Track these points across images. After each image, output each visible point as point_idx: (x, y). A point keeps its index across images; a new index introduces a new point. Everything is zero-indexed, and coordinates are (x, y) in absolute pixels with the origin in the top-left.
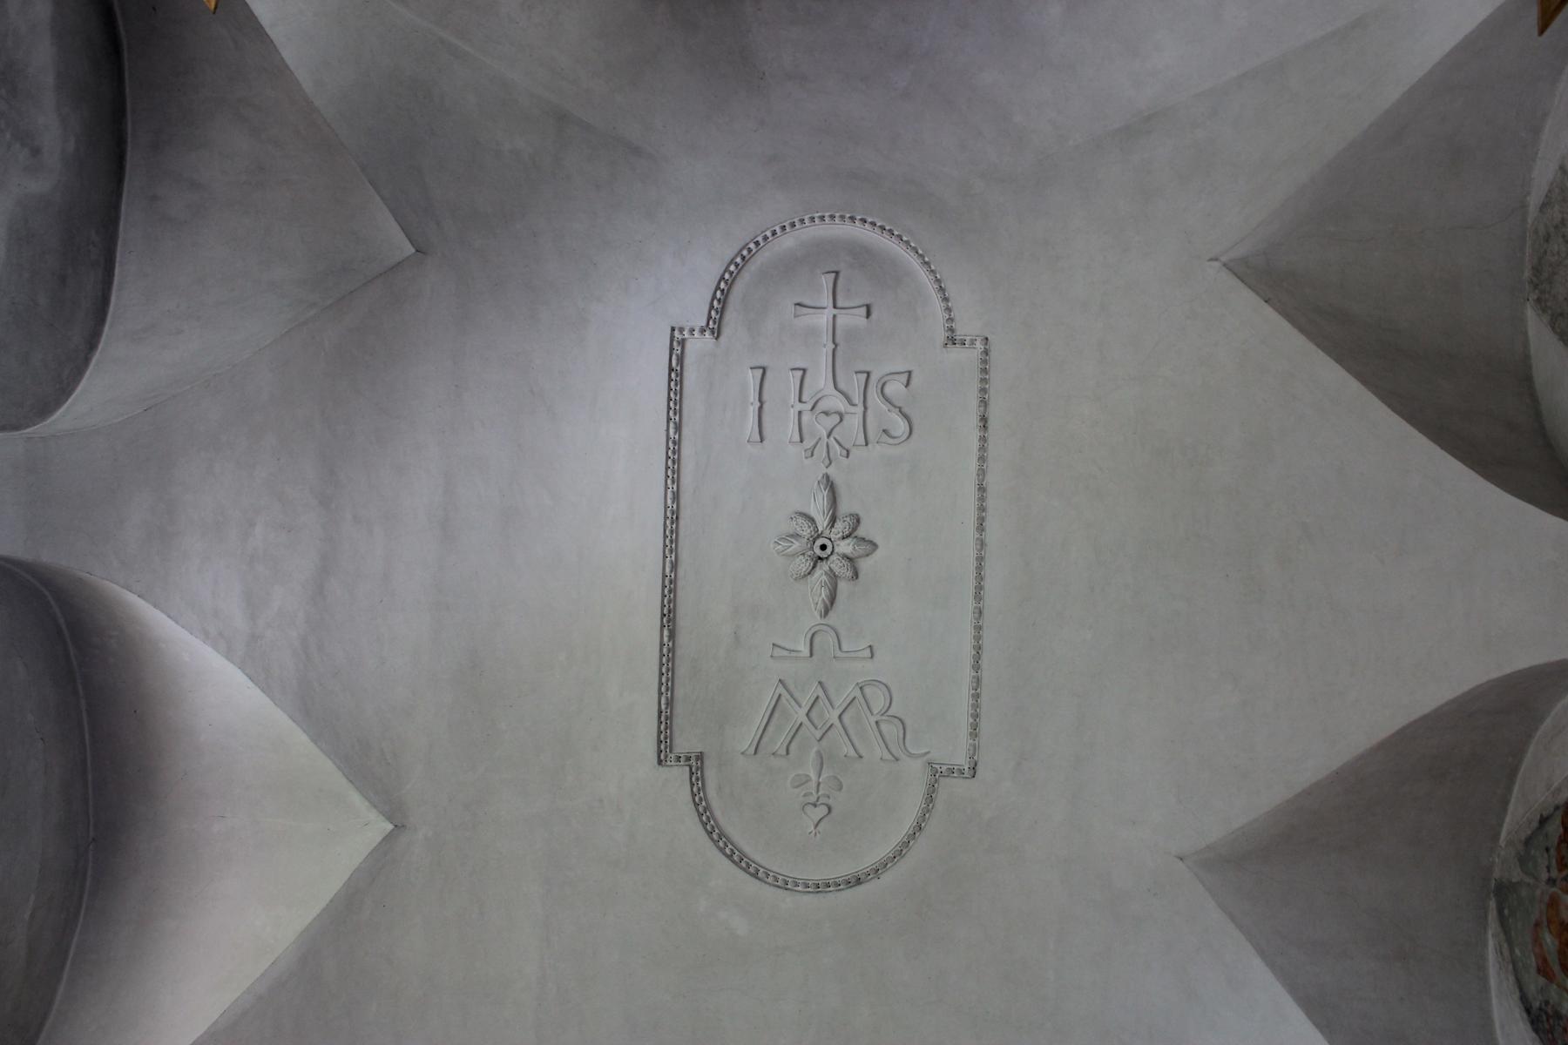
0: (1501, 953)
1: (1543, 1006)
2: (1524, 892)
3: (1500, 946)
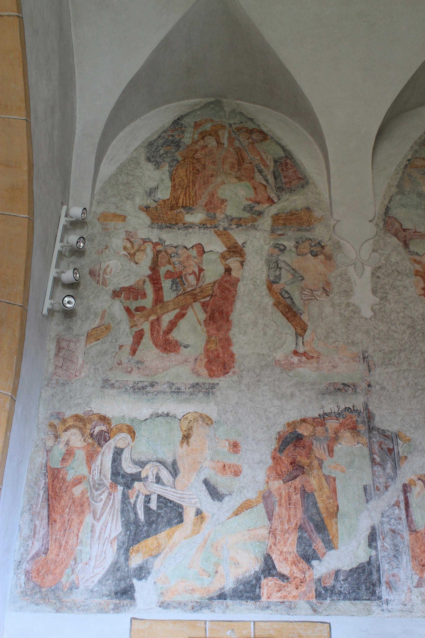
0: (195, 105)
1: (183, 126)
2: (222, 113)
3: (198, 104)
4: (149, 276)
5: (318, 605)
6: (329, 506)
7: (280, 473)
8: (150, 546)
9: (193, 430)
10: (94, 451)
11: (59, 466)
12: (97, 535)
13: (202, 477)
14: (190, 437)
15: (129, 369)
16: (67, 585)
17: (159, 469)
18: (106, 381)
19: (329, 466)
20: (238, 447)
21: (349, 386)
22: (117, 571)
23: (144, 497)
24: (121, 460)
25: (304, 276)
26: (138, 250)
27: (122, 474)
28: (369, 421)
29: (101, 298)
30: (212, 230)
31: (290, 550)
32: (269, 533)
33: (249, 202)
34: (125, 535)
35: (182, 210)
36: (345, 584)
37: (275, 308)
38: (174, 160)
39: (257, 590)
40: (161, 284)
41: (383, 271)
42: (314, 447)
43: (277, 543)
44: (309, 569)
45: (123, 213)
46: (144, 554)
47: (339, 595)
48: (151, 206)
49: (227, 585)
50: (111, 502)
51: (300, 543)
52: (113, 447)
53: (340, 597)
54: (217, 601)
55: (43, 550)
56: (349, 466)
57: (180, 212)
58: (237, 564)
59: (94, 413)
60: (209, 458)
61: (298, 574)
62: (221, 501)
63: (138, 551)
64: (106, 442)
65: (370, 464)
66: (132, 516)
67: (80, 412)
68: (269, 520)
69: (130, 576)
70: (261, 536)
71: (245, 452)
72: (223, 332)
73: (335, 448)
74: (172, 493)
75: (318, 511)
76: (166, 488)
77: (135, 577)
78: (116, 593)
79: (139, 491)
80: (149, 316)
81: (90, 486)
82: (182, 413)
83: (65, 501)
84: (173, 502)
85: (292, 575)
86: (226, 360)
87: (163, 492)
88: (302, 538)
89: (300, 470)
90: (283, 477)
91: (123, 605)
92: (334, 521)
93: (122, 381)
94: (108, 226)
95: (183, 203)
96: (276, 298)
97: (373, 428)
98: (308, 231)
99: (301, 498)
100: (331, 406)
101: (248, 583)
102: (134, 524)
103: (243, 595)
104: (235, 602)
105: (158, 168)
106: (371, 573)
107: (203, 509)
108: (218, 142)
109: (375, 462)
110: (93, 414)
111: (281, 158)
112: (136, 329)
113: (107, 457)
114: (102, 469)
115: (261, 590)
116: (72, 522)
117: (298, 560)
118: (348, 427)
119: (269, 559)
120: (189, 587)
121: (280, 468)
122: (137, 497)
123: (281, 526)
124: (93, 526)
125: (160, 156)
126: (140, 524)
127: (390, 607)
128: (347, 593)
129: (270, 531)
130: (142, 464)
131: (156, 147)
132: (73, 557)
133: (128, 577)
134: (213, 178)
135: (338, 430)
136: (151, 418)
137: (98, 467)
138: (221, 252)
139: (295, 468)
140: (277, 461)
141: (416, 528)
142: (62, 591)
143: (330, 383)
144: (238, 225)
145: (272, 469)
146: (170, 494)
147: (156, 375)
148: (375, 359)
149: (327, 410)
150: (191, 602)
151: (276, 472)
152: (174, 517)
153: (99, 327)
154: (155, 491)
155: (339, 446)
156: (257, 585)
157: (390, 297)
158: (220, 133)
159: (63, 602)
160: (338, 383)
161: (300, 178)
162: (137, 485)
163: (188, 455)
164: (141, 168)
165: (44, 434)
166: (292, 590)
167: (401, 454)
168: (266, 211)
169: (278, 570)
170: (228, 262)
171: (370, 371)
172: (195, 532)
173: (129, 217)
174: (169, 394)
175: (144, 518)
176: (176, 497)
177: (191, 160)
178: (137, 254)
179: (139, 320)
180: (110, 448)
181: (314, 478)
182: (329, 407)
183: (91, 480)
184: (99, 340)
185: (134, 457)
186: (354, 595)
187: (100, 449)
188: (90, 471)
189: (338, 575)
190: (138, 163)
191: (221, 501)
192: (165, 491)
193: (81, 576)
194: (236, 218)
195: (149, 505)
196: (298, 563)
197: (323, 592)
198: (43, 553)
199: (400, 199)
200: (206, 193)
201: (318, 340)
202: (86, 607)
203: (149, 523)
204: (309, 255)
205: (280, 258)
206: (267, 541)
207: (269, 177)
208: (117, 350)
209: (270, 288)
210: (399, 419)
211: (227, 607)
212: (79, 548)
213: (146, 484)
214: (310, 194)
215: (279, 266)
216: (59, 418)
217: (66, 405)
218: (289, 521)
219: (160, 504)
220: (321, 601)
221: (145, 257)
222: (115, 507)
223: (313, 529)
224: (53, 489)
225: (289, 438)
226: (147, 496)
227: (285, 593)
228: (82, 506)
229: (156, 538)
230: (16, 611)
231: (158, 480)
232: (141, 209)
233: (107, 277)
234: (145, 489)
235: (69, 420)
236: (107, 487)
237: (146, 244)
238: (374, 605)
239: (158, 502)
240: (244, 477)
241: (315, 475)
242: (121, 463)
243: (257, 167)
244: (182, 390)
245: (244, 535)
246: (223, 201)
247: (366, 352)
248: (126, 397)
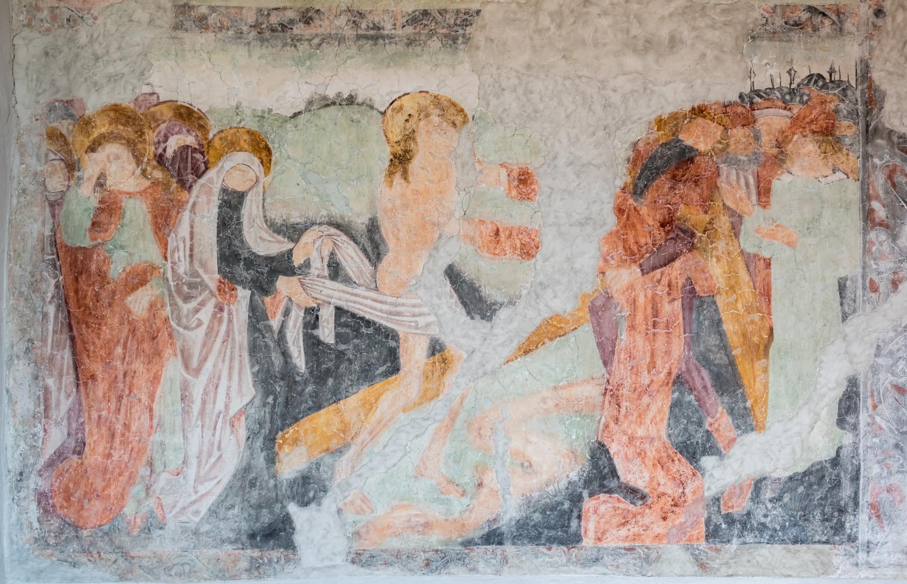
5: (711, 554)
6: (750, 328)
7: (635, 248)
8: (325, 429)
9: (418, 139)
10: (172, 201)
11: (87, 243)
12: (196, 408)
13: (443, 264)
14: (409, 160)
16: (138, 520)
17: (335, 244)
19: (757, 231)
20: (531, 184)
21: (824, 15)
22: (251, 487)
23: (302, 314)
24: (240, 224)
27: (245, 259)
28: (868, 113)
31: (653, 432)
32: (605, 394)
34: (264, 406)
36: (775, 508)
39: (572, 524)
42: (722, 183)
43: (621, 417)
44: (694, 475)
46: (310, 447)
47: (761, 531)
49: (505, 513)
50: (224, 327)
51: (676, 417)
52: (216, 189)
53: (761, 537)
54: (484, 547)
55: (73, 444)
56: (808, 229)
58: (527, 466)
59: (161, 100)
60: (458, 214)
61: (670, 488)
62: (490, 319)
63: (295, 441)
64: (199, 176)
65: (860, 224)
66: (277, 360)
67: (124, 97)
68: (605, 363)
69: (280, 498)
70: (583, 402)
71: (549, 196)
73: (776, 185)
74: (369, 302)
75: (722, 340)
76: (355, 291)
77: (293, 498)
78: (252, 536)
79: (290, 299)
81: (170, 291)
82: (388, 94)
83: (111, 329)
84: (374, 323)
85: (655, 490)
87: (347, 301)
88: (681, 406)
89: (683, 239)
90: (642, 257)
91: (270, 561)
92: (759, 364)
93: (227, 8)
97: (876, 129)
99: (683, 309)
100: (774, 71)
101: (553, 509)
102: (282, 379)
103: (540, 533)
104: (523, 549)
106: (837, 485)
107: (447, 340)
109: (873, 221)
110: (159, 104)
113: (203, 217)
114: (196, 245)
115: (583, 523)
116: (133, 377)
117: (669, 456)
118: (813, 127)
119: (601, 454)
120: (417, 519)
121: (635, 236)
122: (287, 313)
123: (634, 376)
124: (185, 387)
126: (298, 379)
127: (873, 558)
128: (778, 528)
129: (606, 389)
130: (294, 232)
132: (144, 461)
133: (277, 500)
135: (786, 137)
136: (308, 110)
137: (184, 242)
139: (672, 235)
140: (628, 217)
142: (129, 534)
143: (775, 7)
145: (615, 239)
146: (366, 306)
149: (762, 83)
150: (424, 552)
151: (624, 247)
152: (378, 359)
154: (329, 300)
155: (786, 178)
156: (572, 511)
159: (133, 558)
160: (795, 6)
162: (283, 284)
163: (406, 206)
165: (39, 160)
166: (652, 523)
169: (622, 479)
172: (428, 396)
174: (352, 43)
176: (381, 311)
180: (209, 192)
181: (718, 260)
182: (768, 73)
183: (169, 275)
185: (271, 215)
186: (794, 531)
187: (184, 195)
188: (165, 253)
189: (760, 489)
191: (490, 319)
192: (353, 298)
193: (167, 501)
195: (315, 332)
196: (670, 464)
197: (723, 526)
198: (74, 453)
202: (187, 568)
203: (319, 376)
206: (597, 413)
211: (505, 560)
212: (156, 437)
213: (306, 281)
216: (71, 116)
217: (86, 80)
218: (652, 365)
220: (719, 546)
222: (233, 339)
223: (709, 385)
224: (78, 300)
225: (661, 158)
226: (309, 311)
228: (154, 338)
229: (338, 411)
230: (28, 580)
231: (335, 270)
234: (304, 294)
235: (98, 122)
236: (211, 291)
238: (837, 555)
239: (338, 324)
240: (546, 260)
241: (719, 253)
242: (240, 231)
244: (386, 32)
245: (544, 400)
248: (240, 53)
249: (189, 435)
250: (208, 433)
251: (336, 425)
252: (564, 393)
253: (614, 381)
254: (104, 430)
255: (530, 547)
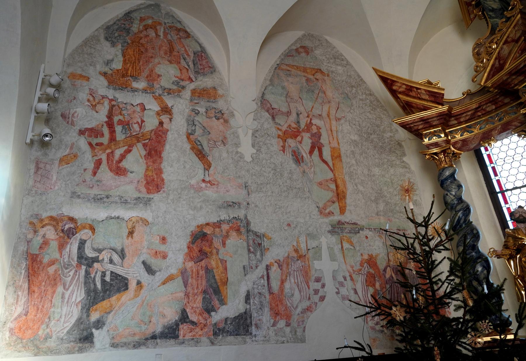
2: (160, 14)
4: (106, 122)
5: (214, 339)
7: (192, 257)
11: (37, 253)
12: (66, 300)
13: (142, 259)
14: (133, 233)
15: (91, 186)
16: (43, 336)
18: (74, 193)
24: (84, 248)
25: (211, 132)
26: (98, 103)
28: (247, 226)
29: (70, 134)
30: (151, 95)
31: (198, 306)
33: (177, 79)
35: (131, 79)
37: (191, 151)
38: (125, 42)
40: (115, 128)
41: (259, 133)
45: (87, 75)
46: (101, 311)
47: (227, 333)
48: (108, 73)
50: (77, 277)
52: (79, 238)
57: (129, 79)
58: (164, 316)
60: (146, 247)
61: (202, 321)
62: (154, 275)
63: (96, 310)
64: (74, 236)
65: (247, 252)
66: (92, 286)
67: (54, 214)
68: (185, 287)
72: (157, 164)
73: (227, 242)
74: (120, 270)
80: (106, 149)
81: (61, 266)
84: (122, 276)
86: (159, 183)
91: (85, 347)
92: (225, 287)
94: (76, 83)
95: (131, 73)
96: (192, 145)
97: (249, 230)
98: (214, 102)
104: (162, 340)
105: (113, 46)
106: (246, 319)
107: (142, 281)
108: (157, 34)
109: (250, 251)
111: (198, 52)
112: (96, 158)
121: (193, 254)
122: (96, 273)
124: (63, 294)
125: (115, 38)
126: (98, 291)
127: (257, 339)
130: (100, 251)
131: (112, 31)
134: (153, 59)
136: (106, 219)
137: (67, 253)
138: (157, 110)
141: (273, 291)
144: (169, 94)
147: (110, 190)
148: (252, 188)
149: (222, 218)
153: (69, 155)
155: (229, 241)
157: (262, 150)
158: (158, 27)
159: (40, 348)
161: (210, 67)
162: (96, 265)
163: (132, 245)
164: (101, 44)
167: (265, 247)
168: (188, 86)
170: (161, 117)
171: (249, 195)
172: (136, 296)
173: (92, 79)
175: (101, 287)
177: (137, 44)
178: (98, 106)
179: (98, 152)
183: (62, 262)
184: (69, 164)
186: (236, 332)
187: (69, 240)
190: (99, 40)
191: (154, 275)
193: (53, 329)
194: (168, 89)
195: (104, 278)
198: (24, 315)
199: (271, 89)
200: (147, 68)
201: (218, 173)
202: (58, 351)
203: (104, 290)
204: (214, 119)
205: (195, 118)
207: (190, 63)
208: (83, 172)
209: (188, 138)
210: (265, 225)
211: (157, 344)
212: (52, 310)
214: (216, 78)
215: (195, 124)
216: (37, 218)
218: (197, 288)
219: (112, 278)
221: (103, 108)
222: (80, 280)
223: (212, 292)
226: (103, 272)
227: (194, 333)
228: (55, 280)
229: (109, 301)
230: (2, 358)
231: (111, 261)
232: (100, 73)
233: (74, 119)
237: (104, 99)
238: (248, 339)
239: (111, 276)
242: (84, 250)
243: (182, 56)
246: (159, 76)
247: (247, 183)
248: (89, 204)
249: (63, 309)
250: (69, 308)
251: (109, 305)
252: (174, 295)
253: (188, 291)
254: (35, 308)
255: (164, 340)
